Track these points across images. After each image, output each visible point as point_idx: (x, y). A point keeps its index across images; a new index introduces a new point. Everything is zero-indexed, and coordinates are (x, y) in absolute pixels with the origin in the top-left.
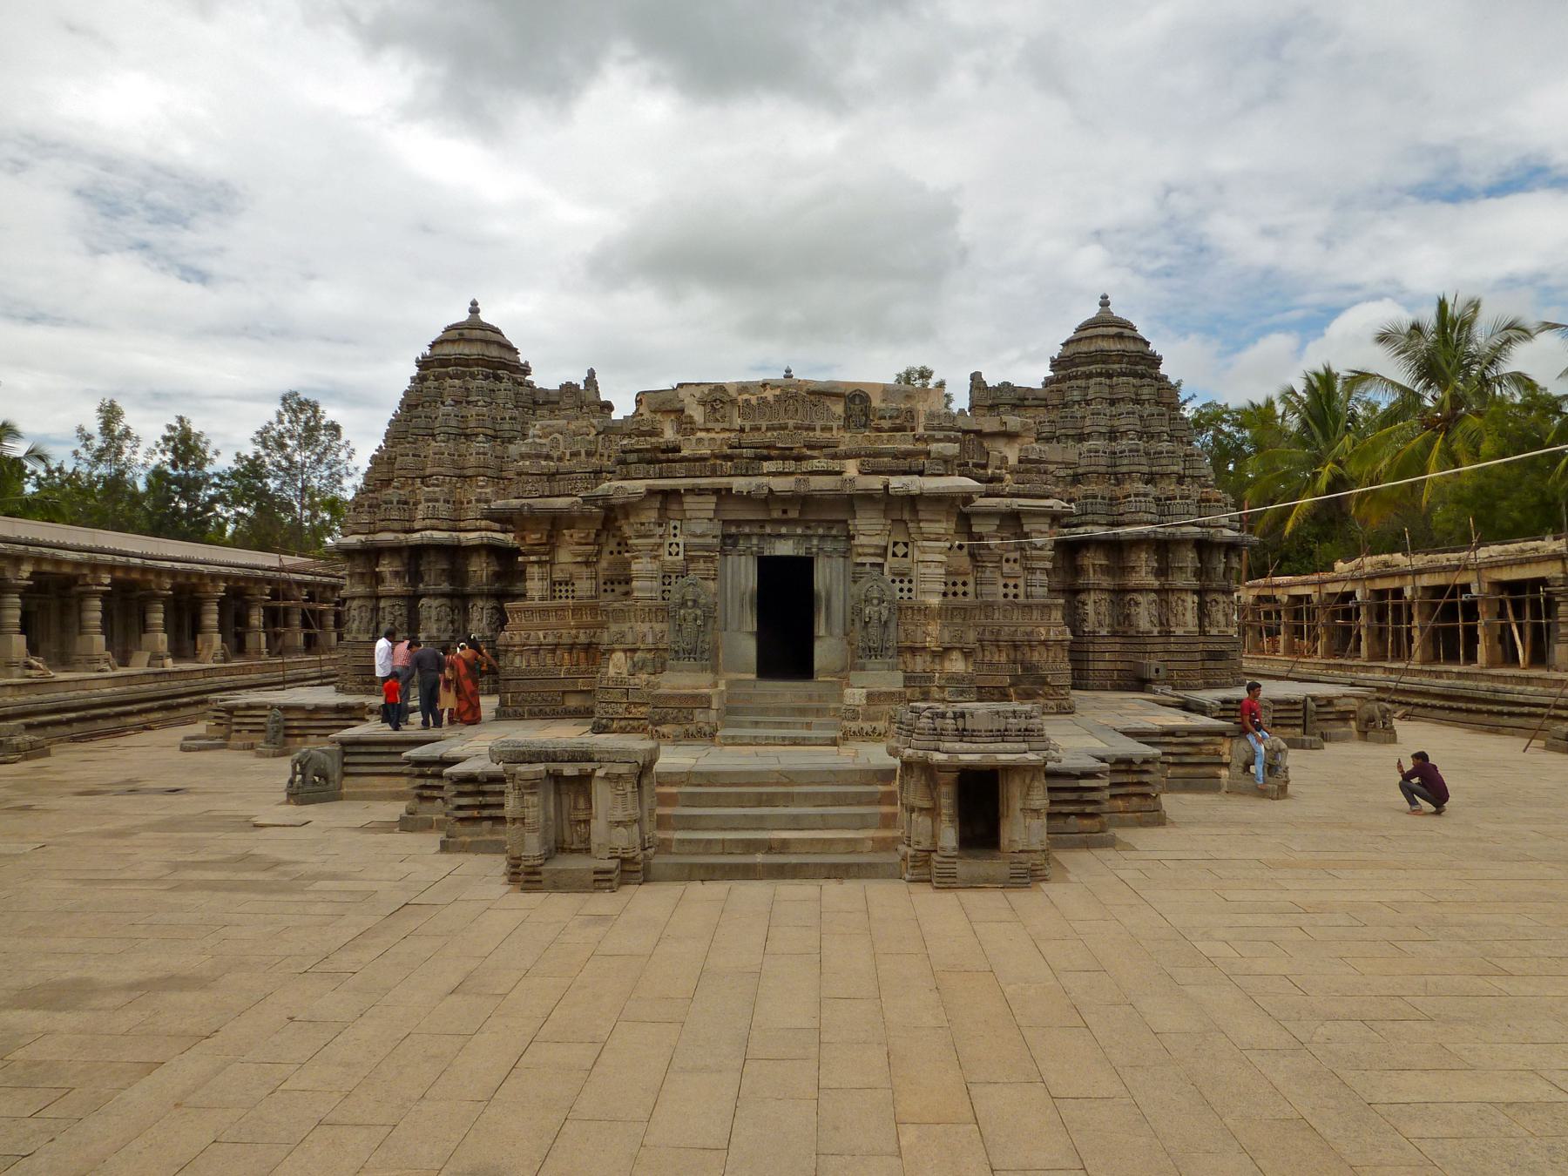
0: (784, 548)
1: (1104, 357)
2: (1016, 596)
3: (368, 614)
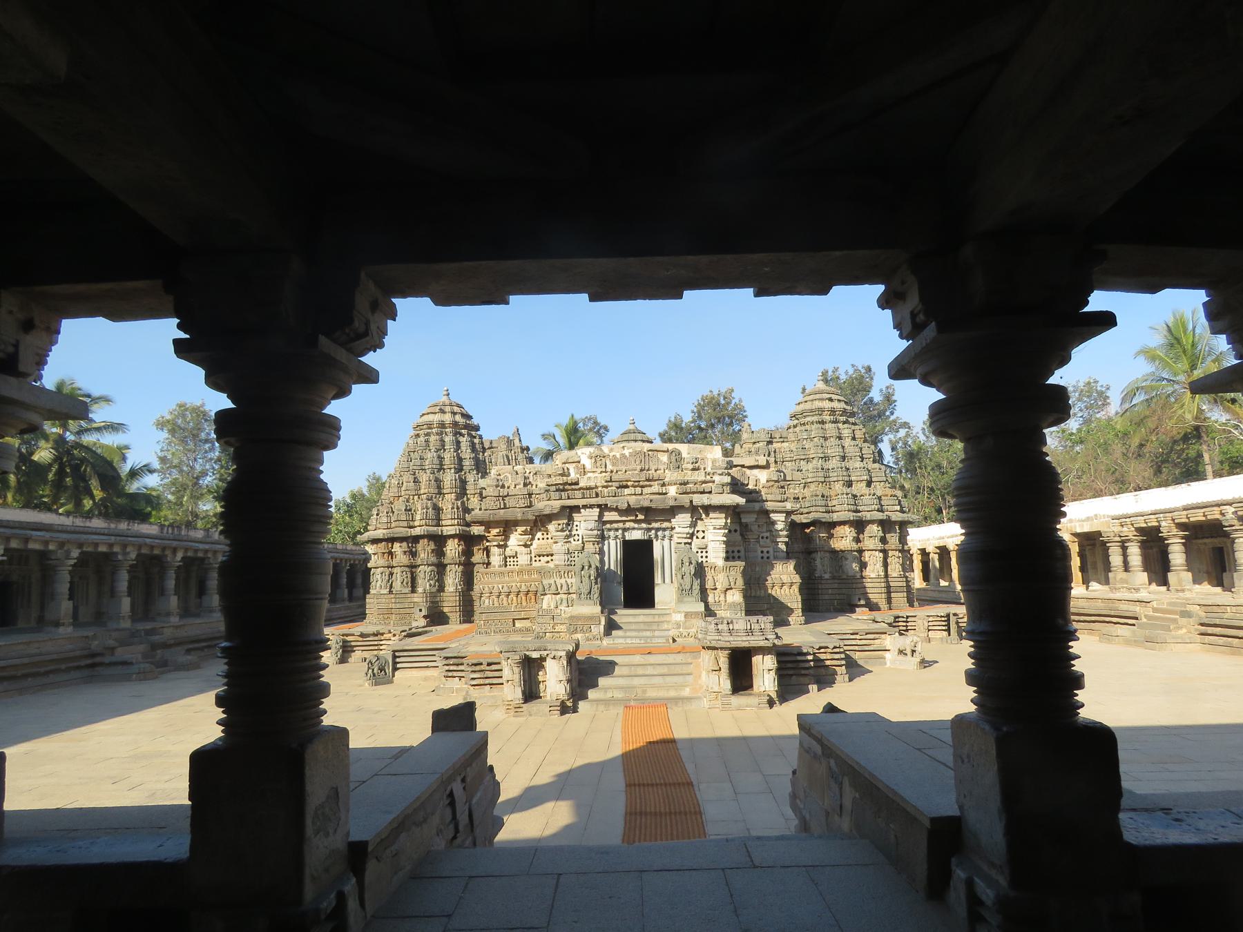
0: (636, 535)
1: (821, 411)
2: (768, 558)
3: (387, 576)
